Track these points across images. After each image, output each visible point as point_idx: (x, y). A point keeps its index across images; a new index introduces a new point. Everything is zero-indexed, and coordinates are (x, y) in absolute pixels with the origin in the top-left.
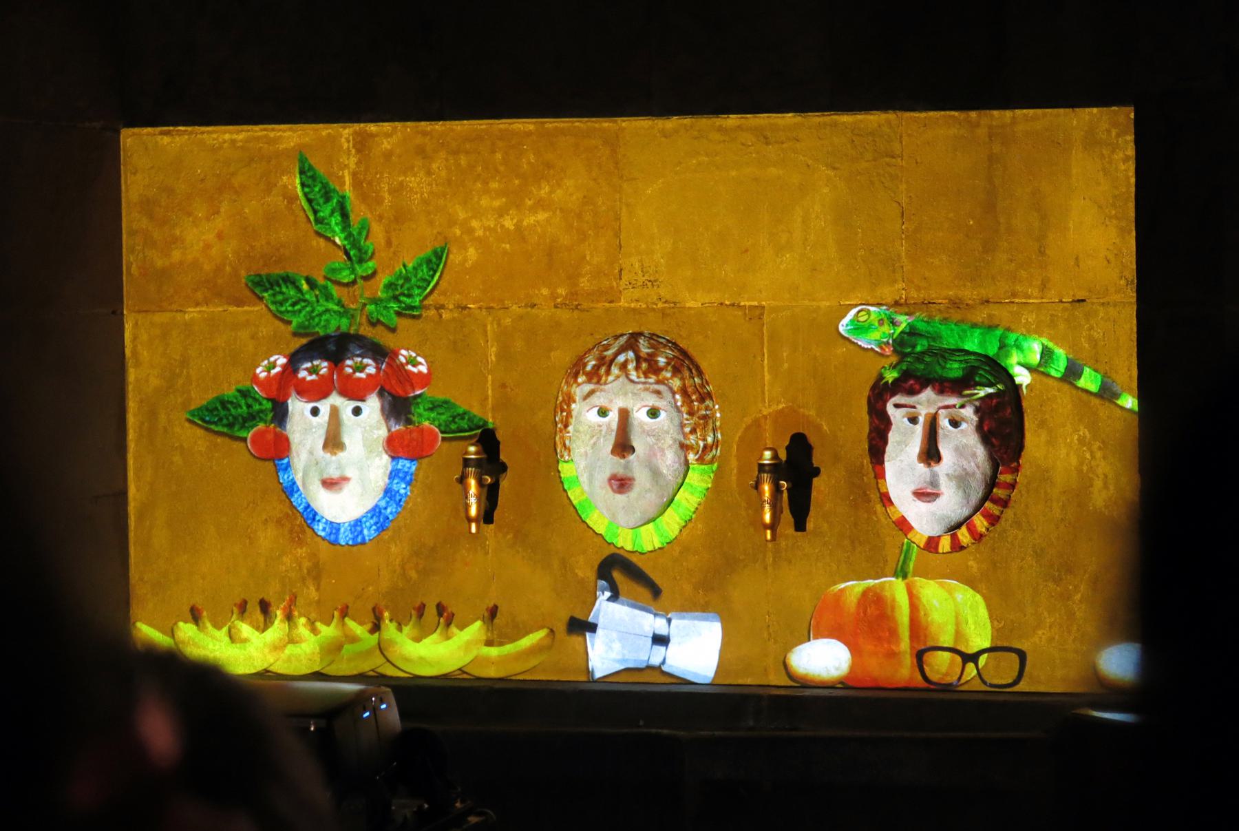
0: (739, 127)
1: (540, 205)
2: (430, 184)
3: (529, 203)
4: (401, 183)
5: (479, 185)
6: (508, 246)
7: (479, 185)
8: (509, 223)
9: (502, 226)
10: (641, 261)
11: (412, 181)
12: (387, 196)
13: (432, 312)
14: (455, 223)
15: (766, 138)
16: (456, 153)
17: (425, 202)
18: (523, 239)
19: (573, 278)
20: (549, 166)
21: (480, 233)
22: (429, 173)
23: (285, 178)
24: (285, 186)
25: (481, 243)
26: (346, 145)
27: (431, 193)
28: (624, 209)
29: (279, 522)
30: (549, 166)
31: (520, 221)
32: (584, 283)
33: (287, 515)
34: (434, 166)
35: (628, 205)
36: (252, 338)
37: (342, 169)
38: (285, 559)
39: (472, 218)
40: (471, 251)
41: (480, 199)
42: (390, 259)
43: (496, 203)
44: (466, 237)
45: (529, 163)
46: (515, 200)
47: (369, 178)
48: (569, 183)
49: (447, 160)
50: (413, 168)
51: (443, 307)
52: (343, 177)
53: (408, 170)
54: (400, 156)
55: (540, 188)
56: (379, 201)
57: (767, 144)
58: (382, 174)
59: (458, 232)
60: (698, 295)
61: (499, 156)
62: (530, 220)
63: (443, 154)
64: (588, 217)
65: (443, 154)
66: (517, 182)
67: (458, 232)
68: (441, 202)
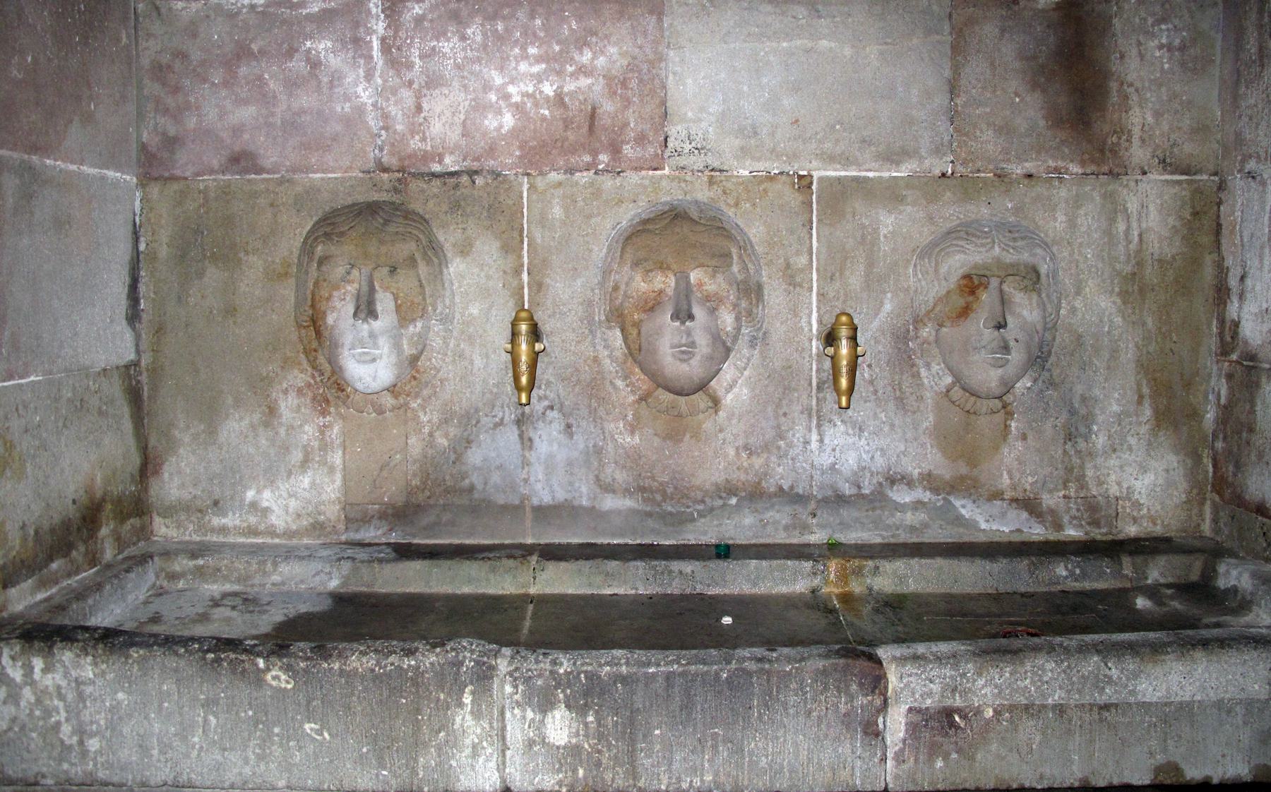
1: (582, 71)
2: (464, 49)
3: (570, 69)
5: (517, 50)
6: (547, 112)
7: (517, 50)
8: (548, 89)
9: (541, 92)
10: (687, 129)
11: (445, 46)
12: (417, 60)
13: (465, 178)
14: (491, 89)
15: (818, 11)
17: (458, 67)
21: (516, 99)
22: (463, 38)
23: (308, 44)
25: (518, 108)
26: (374, 11)
27: (465, 57)
28: (671, 77)
29: (300, 392)
31: (561, 87)
32: (627, 150)
33: (309, 385)
35: (674, 74)
36: (272, 205)
37: (370, 34)
38: (306, 428)
39: (508, 84)
41: (518, 63)
45: (570, 28)
49: (482, 25)
50: (445, 34)
51: (476, 172)
52: (371, 41)
53: (440, 34)
54: (431, 21)
55: (581, 53)
56: (410, 66)
57: (820, 17)
58: (412, 38)
59: (493, 98)
60: (747, 164)
61: (538, 22)
63: (478, 20)
64: (633, 84)
65: (478, 20)
66: (557, 48)
67: (493, 98)
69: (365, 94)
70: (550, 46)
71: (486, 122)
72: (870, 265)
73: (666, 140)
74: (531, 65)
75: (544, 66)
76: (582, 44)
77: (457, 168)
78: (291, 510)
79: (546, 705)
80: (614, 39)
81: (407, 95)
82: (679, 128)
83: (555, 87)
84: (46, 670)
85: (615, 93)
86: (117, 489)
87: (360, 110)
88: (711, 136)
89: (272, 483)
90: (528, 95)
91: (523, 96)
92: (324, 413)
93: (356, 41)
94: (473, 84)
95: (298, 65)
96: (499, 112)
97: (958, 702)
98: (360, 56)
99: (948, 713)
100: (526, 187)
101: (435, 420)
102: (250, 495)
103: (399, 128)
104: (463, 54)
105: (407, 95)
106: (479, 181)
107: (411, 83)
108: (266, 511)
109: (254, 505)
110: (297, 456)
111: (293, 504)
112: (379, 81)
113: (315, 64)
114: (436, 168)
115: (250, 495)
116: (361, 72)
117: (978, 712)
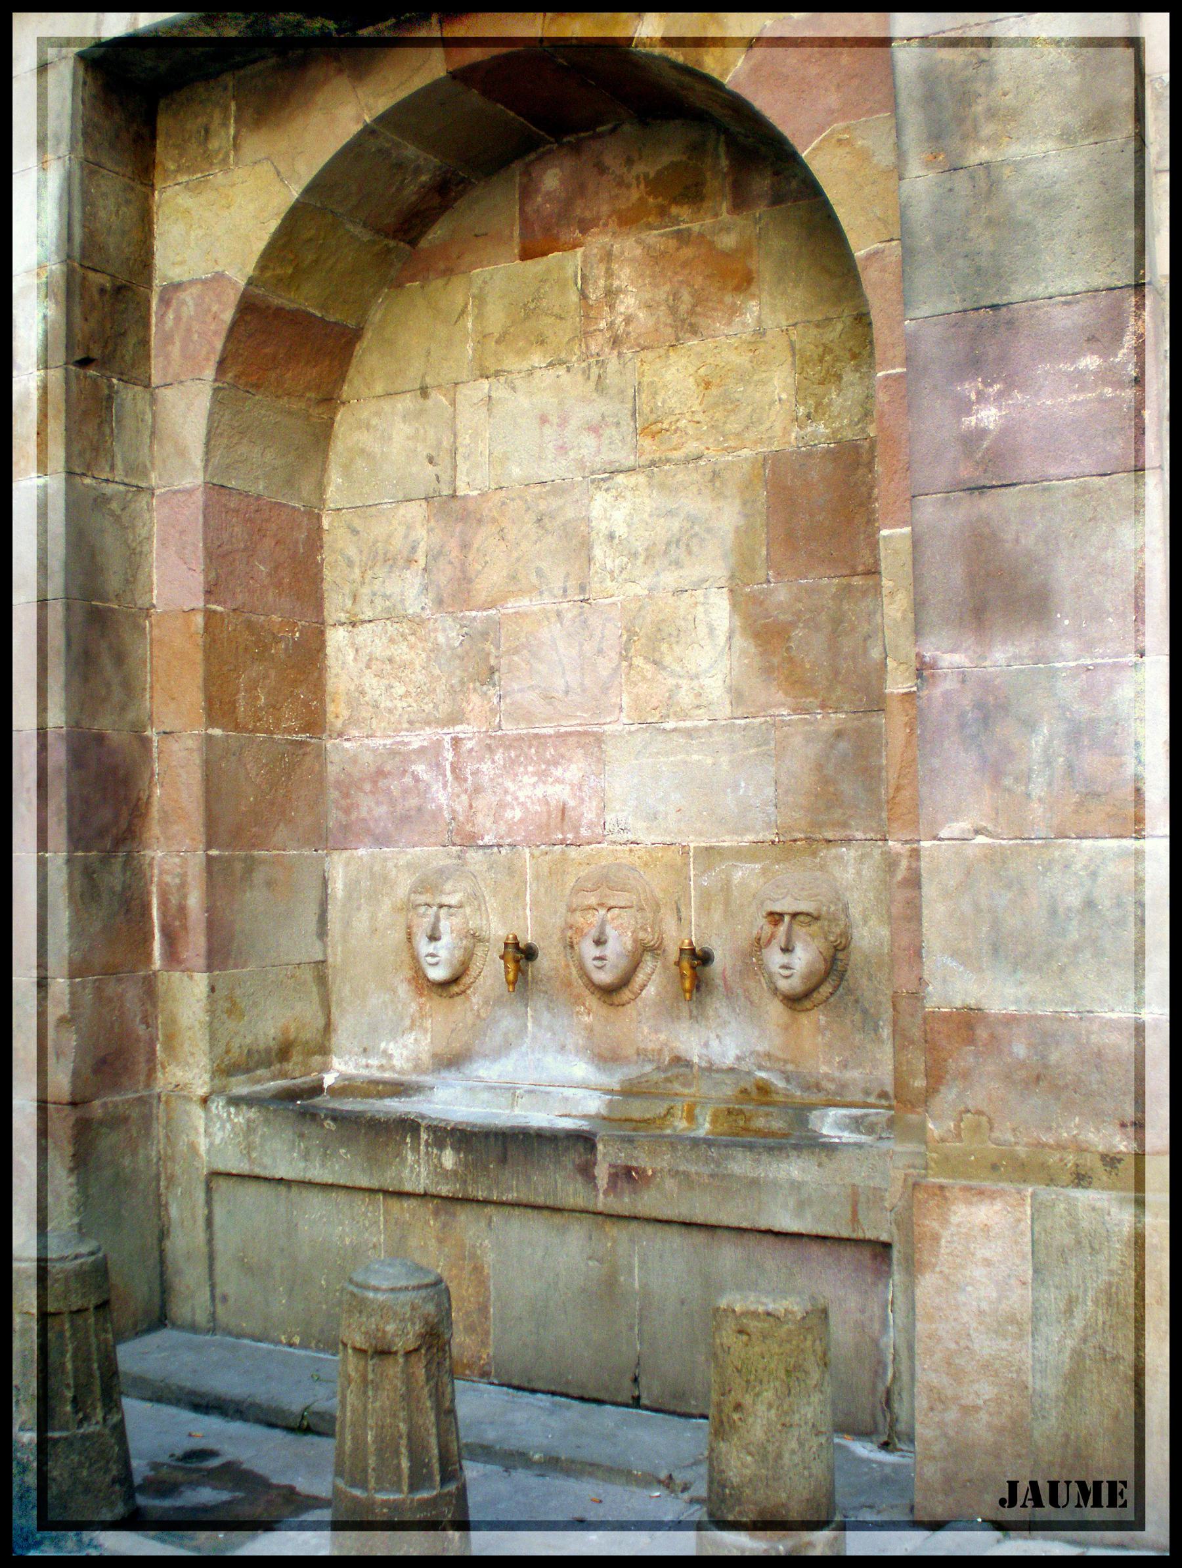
0: (675, 730)
1: (558, 781)
8: (539, 792)
16: (509, 747)
17: (492, 780)
18: (547, 803)
19: (576, 829)
20: (562, 756)
21: (522, 800)
22: (493, 762)
30: (562, 756)
46: (542, 776)
48: (573, 767)
53: (481, 760)
56: (466, 780)
62: (550, 790)
64: (585, 788)
69: (442, 798)
72: (727, 903)
76: (556, 764)
79: (441, 1147)
84: (237, 1115)
86: (306, 1035)
88: (630, 821)
89: (394, 1039)
92: (421, 995)
93: (438, 765)
94: (499, 791)
95: (408, 780)
97: (635, 1164)
99: (628, 1170)
100: (528, 856)
102: (383, 1045)
105: (464, 797)
106: (503, 851)
108: (391, 1056)
109: (385, 1052)
110: (408, 1022)
111: (405, 1053)
113: (417, 779)
114: (480, 843)
115: (383, 1045)
117: (644, 1171)
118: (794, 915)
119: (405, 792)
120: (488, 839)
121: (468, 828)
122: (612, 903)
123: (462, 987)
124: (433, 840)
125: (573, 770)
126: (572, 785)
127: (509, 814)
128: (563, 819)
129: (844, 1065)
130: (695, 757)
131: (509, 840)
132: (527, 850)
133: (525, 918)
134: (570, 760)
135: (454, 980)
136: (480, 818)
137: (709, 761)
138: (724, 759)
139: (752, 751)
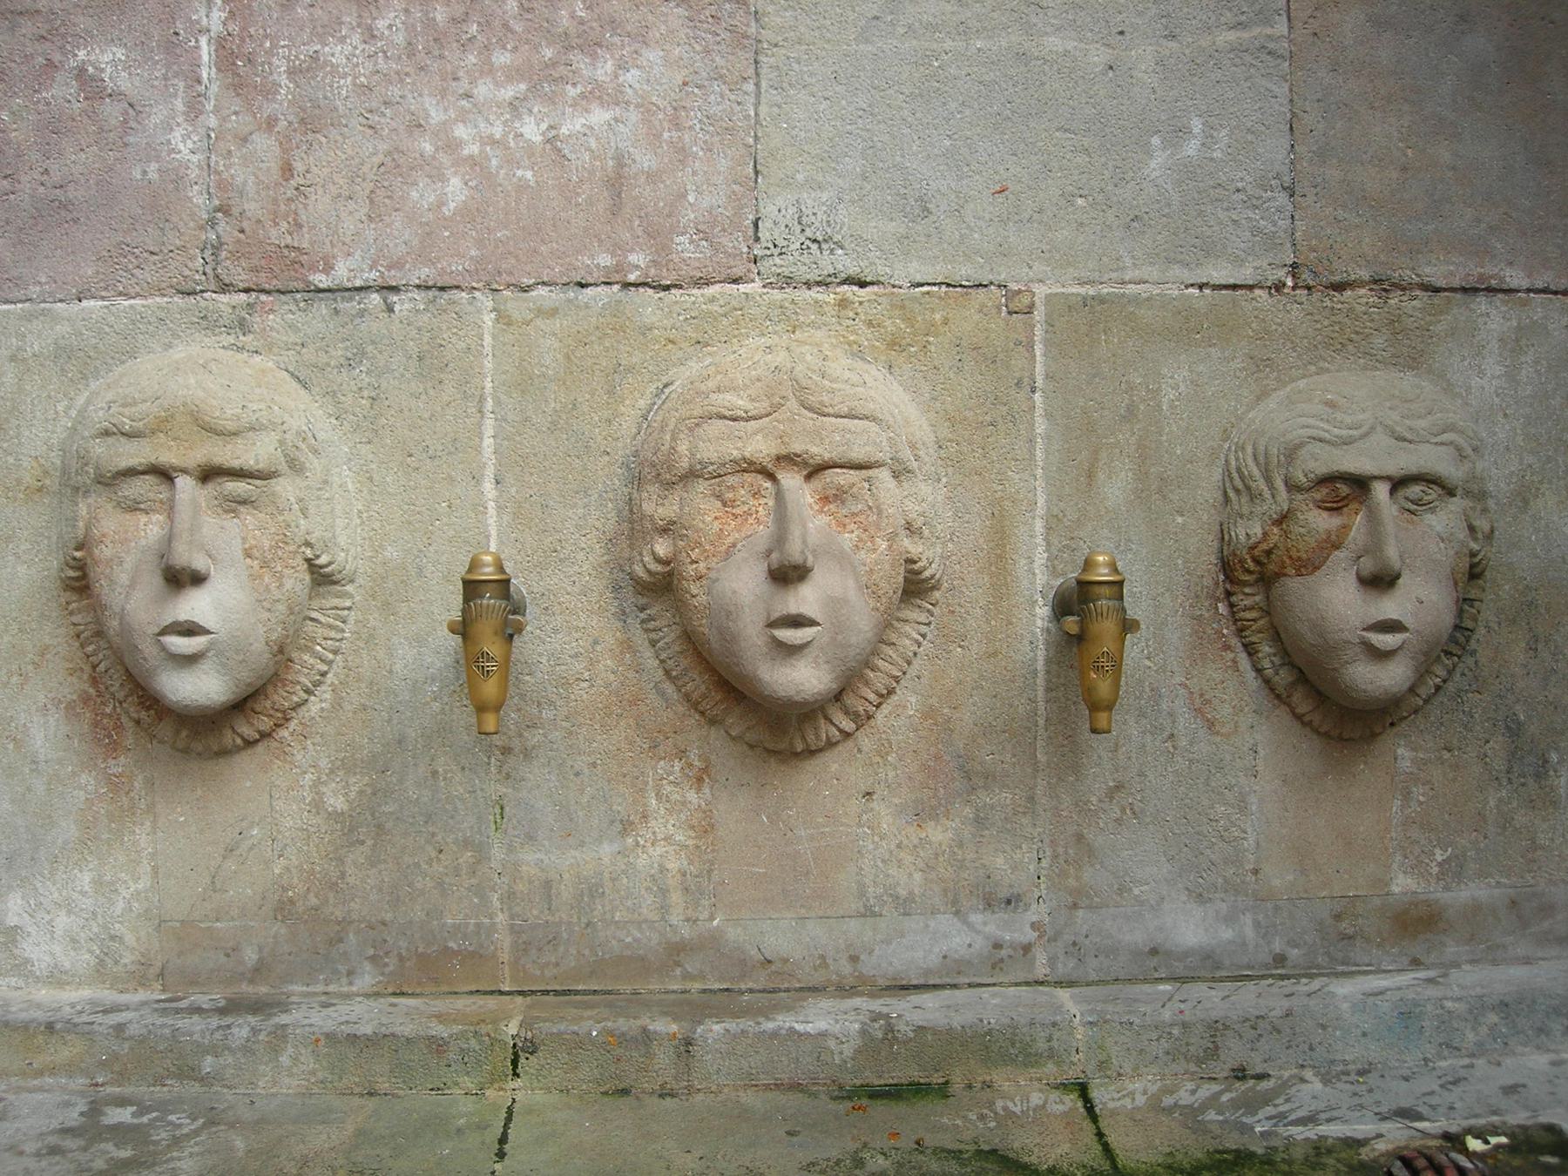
1: (597, 94)
3: (572, 92)
4: (315, 57)
5: (472, 59)
6: (529, 174)
7: (472, 59)
8: (532, 130)
11: (336, 53)
12: (284, 80)
13: (375, 298)
19: (658, 237)
21: (474, 149)
22: (371, 35)
23: (82, 54)
24: (81, 72)
29: (70, 707)
30: (613, 24)
34: (381, 24)
36: (13, 358)
40: (455, 182)
42: (290, 200)
43: (508, 93)
44: (444, 159)
46: (544, 82)
47: (249, 47)
48: (652, 55)
49: (407, 11)
51: (394, 289)
56: (269, 91)
58: (274, 39)
59: (428, 148)
62: (572, 125)
67: (428, 148)
68: (395, 91)
69: (184, 145)
70: (536, 48)
71: (414, 194)
73: (756, 226)
74: (497, 84)
75: (523, 87)
76: (592, 46)
77: (358, 283)
78: (59, 932)
80: (654, 34)
81: (263, 144)
82: (780, 202)
83: (544, 126)
85: (658, 136)
87: (176, 178)
88: (843, 214)
90: (493, 142)
91: (483, 144)
92: (113, 748)
93: (172, 45)
95: (62, 91)
96: (439, 177)
98: (176, 75)
100: (488, 319)
101: (324, 763)
103: (252, 208)
104: (370, 65)
105: (263, 144)
107: (271, 123)
110: (68, 829)
112: (213, 122)
116: (179, 105)
118: (1398, 484)
119: (54, 127)
120: (342, 272)
121: (277, 235)
122: (819, 451)
123: (265, 723)
124: (146, 275)
125: (652, 70)
126: (647, 108)
127: (421, 195)
128: (615, 210)
129: (1453, 871)
130: (1054, 43)
131: (425, 273)
132: (485, 301)
133: (479, 508)
134: (642, 38)
135: (242, 705)
136: (320, 204)
137: (1098, 57)
138: (1142, 56)
139: (1228, 37)
